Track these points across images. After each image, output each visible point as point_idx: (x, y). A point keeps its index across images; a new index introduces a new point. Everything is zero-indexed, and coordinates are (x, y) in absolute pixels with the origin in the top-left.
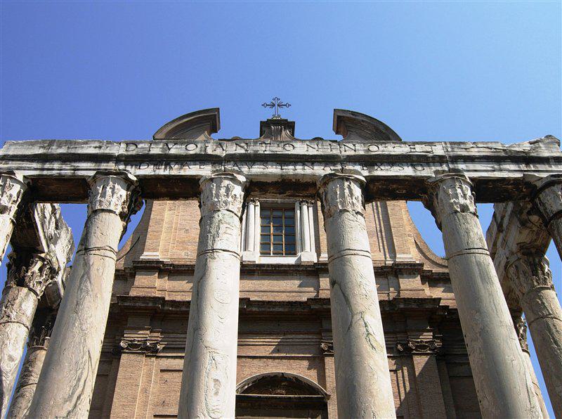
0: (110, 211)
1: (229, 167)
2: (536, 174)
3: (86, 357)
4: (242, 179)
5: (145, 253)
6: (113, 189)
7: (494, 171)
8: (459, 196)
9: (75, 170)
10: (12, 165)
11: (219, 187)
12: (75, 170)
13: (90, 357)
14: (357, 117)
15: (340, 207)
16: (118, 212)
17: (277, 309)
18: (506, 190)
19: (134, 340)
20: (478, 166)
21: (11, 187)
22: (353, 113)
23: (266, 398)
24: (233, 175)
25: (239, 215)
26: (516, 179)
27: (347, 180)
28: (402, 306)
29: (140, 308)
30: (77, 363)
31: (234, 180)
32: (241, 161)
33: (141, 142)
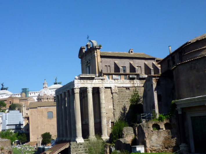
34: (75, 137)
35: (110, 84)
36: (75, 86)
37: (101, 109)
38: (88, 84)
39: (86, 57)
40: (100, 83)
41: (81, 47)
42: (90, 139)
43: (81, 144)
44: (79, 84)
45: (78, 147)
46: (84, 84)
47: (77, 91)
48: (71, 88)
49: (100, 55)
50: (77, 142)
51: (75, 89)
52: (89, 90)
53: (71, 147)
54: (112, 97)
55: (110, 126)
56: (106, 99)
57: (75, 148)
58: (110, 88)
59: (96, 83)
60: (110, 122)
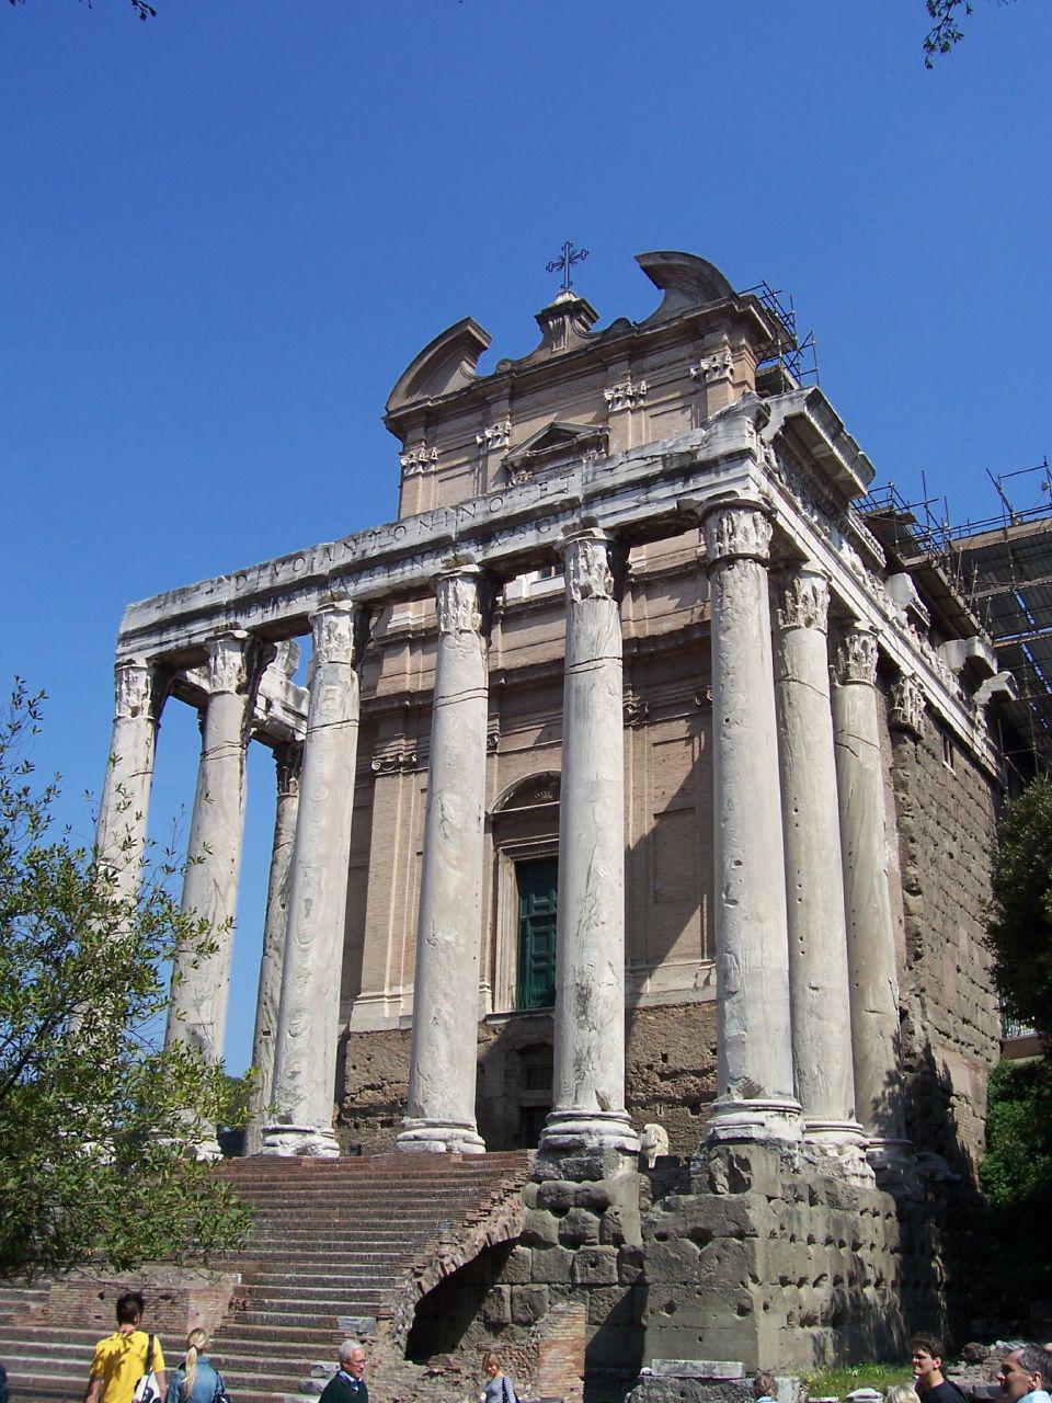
0: (223, 693)
1: (336, 588)
2: (697, 497)
3: (212, 887)
4: (346, 605)
5: (394, 617)
6: (223, 658)
7: (638, 506)
8: (581, 572)
9: (190, 636)
10: (136, 643)
11: (320, 629)
12: (190, 636)
14: (671, 262)
15: (443, 629)
16: (233, 689)
17: (544, 674)
18: (669, 525)
19: (386, 758)
20: (618, 505)
21: (135, 680)
22: (664, 255)
23: (528, 810)
24: (333, 606)
25: (349, 661)
26: (666, 512)
27: (453, 579)
28: (697, 635)
29: (387, 711)
30: (202, 898)
31: (337, 612)
32: (347, 575)
33: (250, 571)
38: (811, 528)
39: (519, 404)
40: (861, 578)
51: (750, 507)
52: (820, 597)
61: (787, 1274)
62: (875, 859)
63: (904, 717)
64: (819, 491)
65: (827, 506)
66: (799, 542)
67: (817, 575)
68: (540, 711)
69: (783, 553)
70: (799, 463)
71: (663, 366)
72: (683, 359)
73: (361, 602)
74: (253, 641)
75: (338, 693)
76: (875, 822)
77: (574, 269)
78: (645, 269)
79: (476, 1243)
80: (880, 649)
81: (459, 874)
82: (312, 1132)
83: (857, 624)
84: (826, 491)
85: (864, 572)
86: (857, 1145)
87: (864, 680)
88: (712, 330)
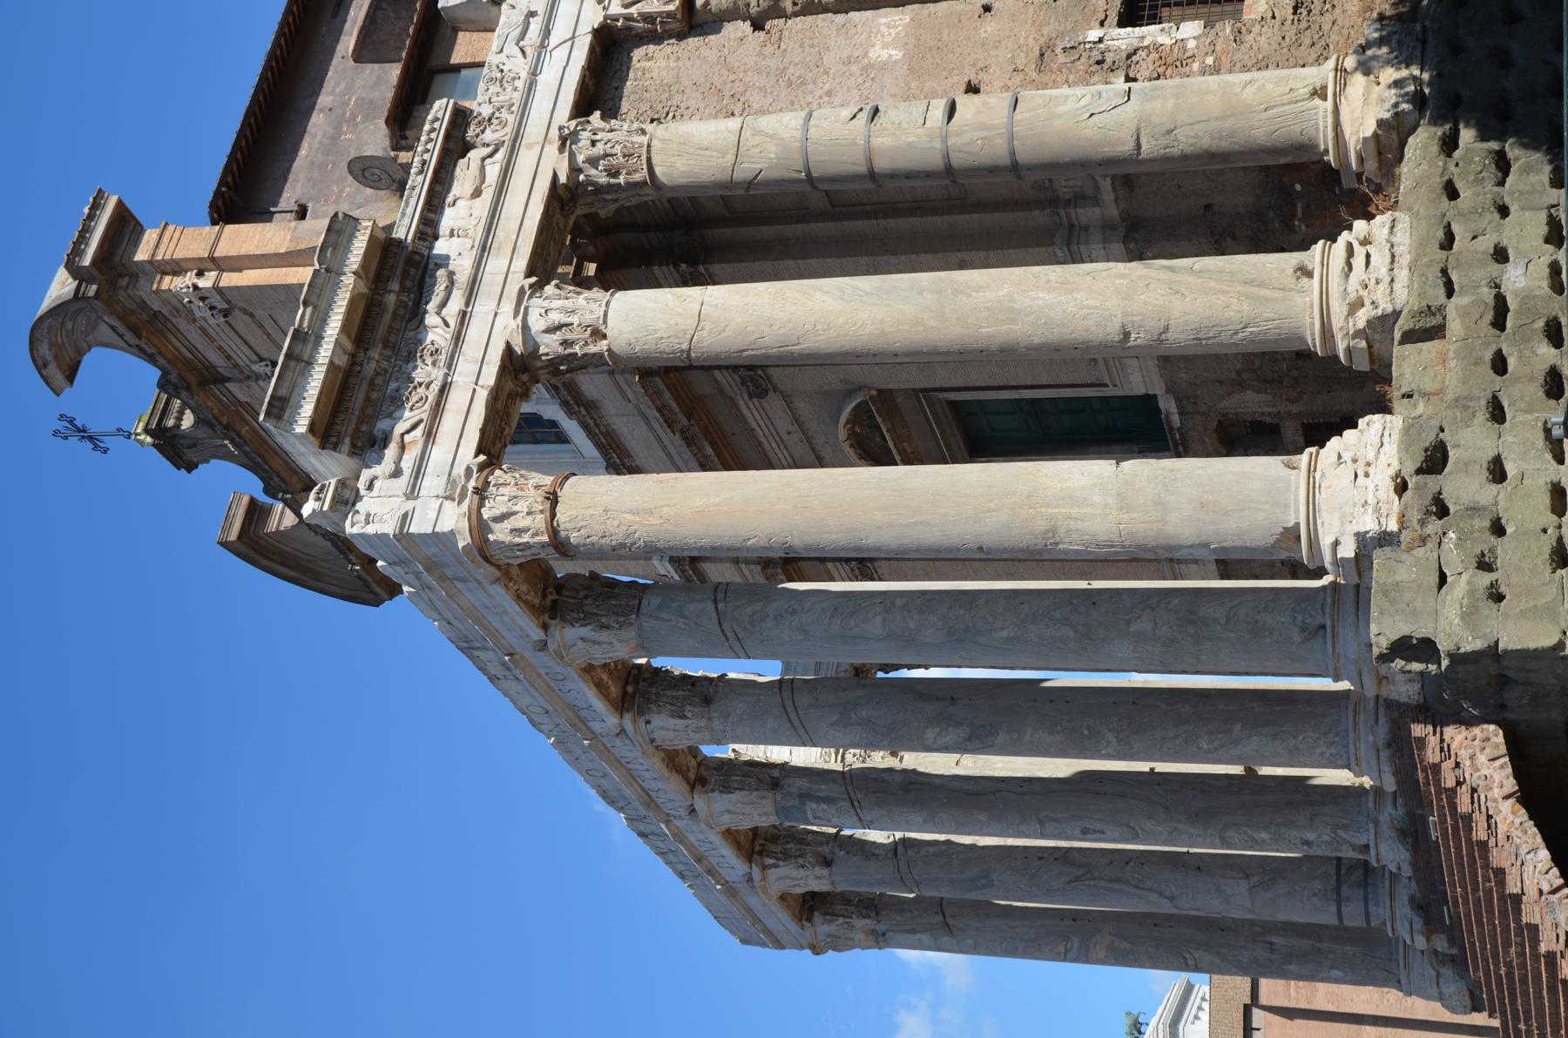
13: (1077, 879)
16: (825, 872)
25: (770, 794)
34: (1287, 556)
35: (554, 39)
36: (445, 526)
37: (882, 164)
38: (458, 339)
40: (493, 171)
41: (224, 544)
42: (1362, 318)
43: (1435, 460)
44: (419, 471)
45: (1474, 510)
46: (445, 389)
47: (517, 504)
48: (537, 634)
49: (214, 223)
50: (1369, 525)
51: (480, 528)
52: (556, 317)
53: (1471, 644)
54: (746, 26)
55: (1191, 29)
56: (755, 99)
57: (1485, 565)
58: (610, 51)
59: (487, 227)
60: (1124, 38)
61: (1547, 551)
62: (910, 145)
63: (669, 14)
64: (395, 313)
65: (409, 284)
66: (490, 377)
67: (525, 327)
68: (760, 444)
69: (510, 385)
70: (372, 384)
71: (220, 348)
72: (203, 329)
73: (692, 787)
74: (761, 853)
75: (814, 806)
76: (855, 144)
77: (94, 428)
78: (71, 378)
79: (1517, 821)
80: (582, 108)
81: (1030, 730)
82: (1376, 823)
83: (563, 179)
84: (391, 299)
85: (475, 155)
86: (1347, 276)
87: (644, 158)
88: (143, 305)
